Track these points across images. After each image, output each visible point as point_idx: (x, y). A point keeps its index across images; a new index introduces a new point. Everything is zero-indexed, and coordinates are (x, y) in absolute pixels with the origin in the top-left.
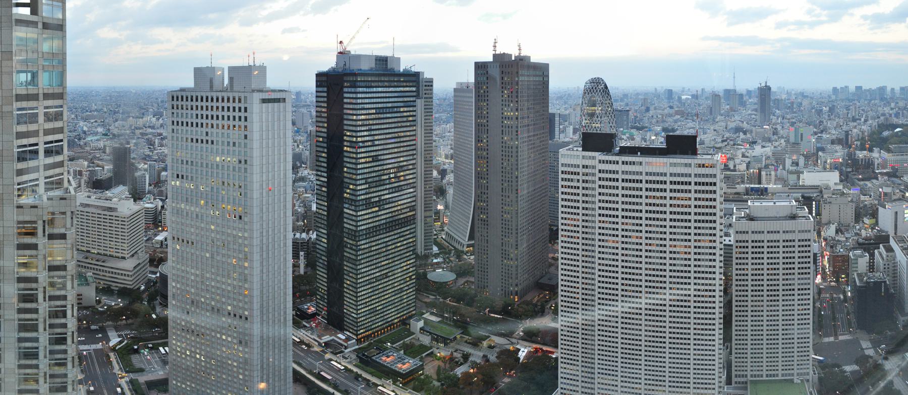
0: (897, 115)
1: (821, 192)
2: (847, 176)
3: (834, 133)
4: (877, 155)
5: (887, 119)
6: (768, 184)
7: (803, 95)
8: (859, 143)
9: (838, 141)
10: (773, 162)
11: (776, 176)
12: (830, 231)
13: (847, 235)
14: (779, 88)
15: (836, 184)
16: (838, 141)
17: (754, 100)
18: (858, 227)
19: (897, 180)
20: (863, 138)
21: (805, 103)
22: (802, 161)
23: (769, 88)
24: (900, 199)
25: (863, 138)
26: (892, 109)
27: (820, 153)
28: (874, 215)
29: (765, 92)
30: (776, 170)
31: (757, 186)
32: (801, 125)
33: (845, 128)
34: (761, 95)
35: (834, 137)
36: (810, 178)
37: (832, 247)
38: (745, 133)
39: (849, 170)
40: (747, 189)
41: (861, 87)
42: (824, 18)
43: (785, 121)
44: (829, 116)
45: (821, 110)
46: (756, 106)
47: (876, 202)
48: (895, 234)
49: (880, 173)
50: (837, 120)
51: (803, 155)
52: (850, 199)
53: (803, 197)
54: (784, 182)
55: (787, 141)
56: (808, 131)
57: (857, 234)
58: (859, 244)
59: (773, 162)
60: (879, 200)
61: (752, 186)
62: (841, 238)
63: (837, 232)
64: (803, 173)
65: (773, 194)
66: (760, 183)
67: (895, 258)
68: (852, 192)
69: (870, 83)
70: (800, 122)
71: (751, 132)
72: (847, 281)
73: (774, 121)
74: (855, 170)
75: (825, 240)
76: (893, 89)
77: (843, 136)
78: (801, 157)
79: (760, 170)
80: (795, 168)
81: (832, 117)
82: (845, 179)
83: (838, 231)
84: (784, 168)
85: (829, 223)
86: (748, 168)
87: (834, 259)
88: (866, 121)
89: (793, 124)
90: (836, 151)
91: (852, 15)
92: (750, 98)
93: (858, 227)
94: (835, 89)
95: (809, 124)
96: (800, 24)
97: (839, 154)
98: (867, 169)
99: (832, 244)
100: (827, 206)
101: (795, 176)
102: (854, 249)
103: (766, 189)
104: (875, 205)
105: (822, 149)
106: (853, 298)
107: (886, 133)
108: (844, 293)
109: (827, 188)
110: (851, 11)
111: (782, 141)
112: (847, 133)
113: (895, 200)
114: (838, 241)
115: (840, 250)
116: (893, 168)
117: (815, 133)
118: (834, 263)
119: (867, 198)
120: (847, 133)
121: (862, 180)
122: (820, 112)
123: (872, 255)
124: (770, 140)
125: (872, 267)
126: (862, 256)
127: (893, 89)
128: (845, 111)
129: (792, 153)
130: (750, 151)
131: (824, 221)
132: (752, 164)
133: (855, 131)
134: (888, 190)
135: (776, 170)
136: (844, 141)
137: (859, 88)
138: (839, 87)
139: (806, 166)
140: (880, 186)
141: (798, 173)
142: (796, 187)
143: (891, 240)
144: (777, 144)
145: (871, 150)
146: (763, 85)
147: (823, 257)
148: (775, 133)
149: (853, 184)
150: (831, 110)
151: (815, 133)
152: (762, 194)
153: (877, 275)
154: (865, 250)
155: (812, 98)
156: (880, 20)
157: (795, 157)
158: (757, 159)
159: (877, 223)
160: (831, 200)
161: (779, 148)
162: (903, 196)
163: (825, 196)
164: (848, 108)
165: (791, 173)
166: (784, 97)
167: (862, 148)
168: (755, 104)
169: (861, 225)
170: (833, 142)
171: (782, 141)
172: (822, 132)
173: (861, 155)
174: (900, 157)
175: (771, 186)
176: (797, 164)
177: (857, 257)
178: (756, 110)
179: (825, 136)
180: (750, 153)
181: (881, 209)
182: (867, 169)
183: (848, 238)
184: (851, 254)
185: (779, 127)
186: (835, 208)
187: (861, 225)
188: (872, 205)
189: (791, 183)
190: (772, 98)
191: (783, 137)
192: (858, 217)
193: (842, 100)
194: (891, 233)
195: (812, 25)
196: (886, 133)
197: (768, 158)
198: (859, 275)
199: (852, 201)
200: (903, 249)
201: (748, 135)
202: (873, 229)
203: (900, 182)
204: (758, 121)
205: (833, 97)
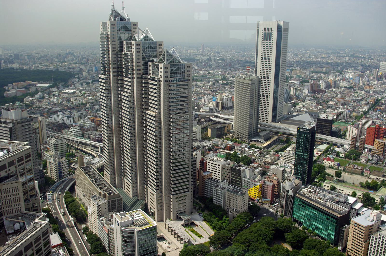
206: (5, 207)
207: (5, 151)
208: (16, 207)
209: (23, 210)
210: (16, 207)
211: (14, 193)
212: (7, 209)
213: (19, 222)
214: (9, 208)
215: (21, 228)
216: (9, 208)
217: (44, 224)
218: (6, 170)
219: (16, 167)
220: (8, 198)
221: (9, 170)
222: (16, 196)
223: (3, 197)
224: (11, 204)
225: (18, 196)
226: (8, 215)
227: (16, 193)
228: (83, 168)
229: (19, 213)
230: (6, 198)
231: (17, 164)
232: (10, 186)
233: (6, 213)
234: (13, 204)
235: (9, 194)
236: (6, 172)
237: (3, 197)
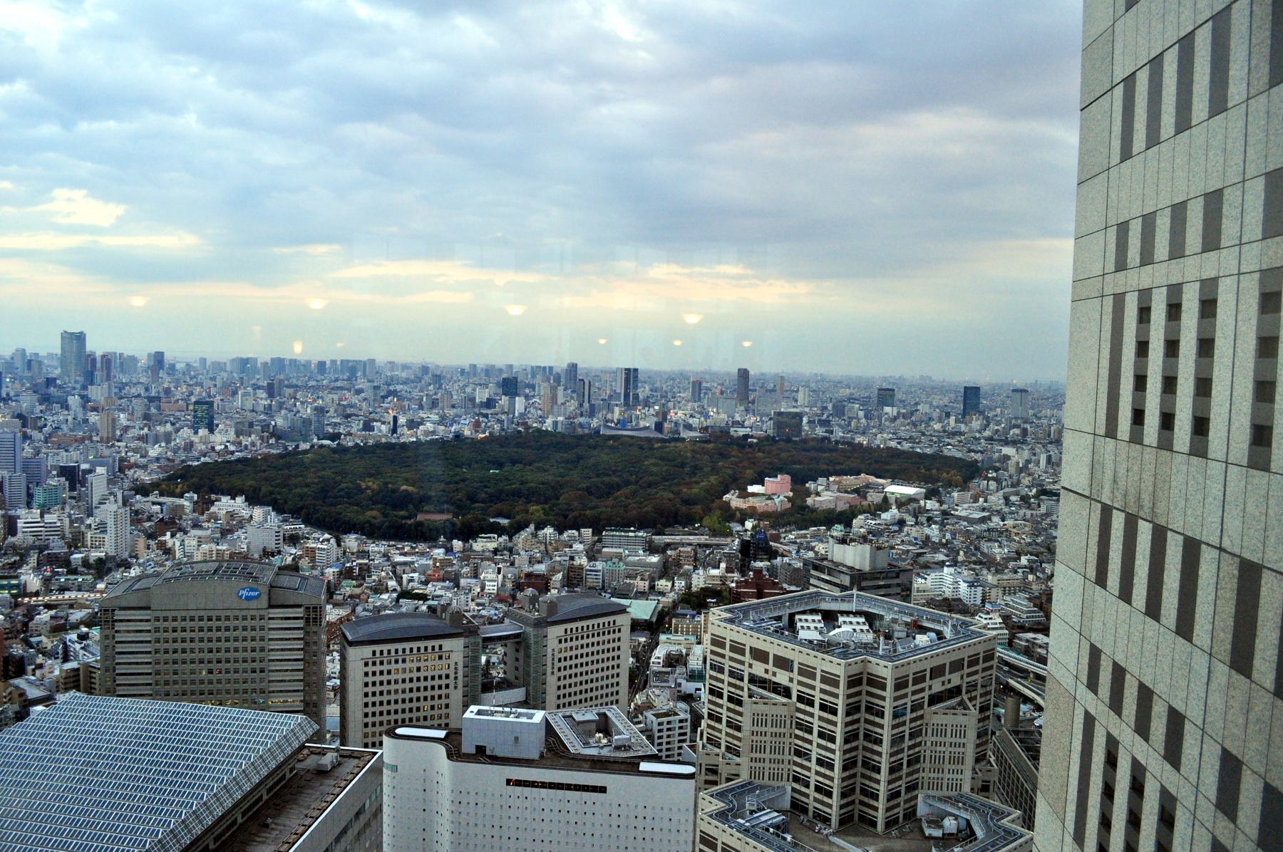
206: (927, 770)
207: (933, 635)
208: (951, 776)
209: (966, 789)
210: (951, 776)
211: (953, 740)
212: (932, 775)
213: (956, 817)
214: (936, 775)
215: (959, 831)
216: (936, 775)
217: (1021, 836)
218: (942, 679)
219: (962, 677)
220: (938, 749)
221: (949, 681)
222: (957, 750)
223: (929, 744)
224: (941, 766)
225: (961, 750)
226: (931, 792)
227: (958, 740)
228: (1016, 733)
229: (953, 793)
230: (933, 748)
231: (966, 671)
232: (949, 720)
233: (926, 786)
234: (947, 766)
235: (943, 739)
236: (943, 683)
237: (929, 744)
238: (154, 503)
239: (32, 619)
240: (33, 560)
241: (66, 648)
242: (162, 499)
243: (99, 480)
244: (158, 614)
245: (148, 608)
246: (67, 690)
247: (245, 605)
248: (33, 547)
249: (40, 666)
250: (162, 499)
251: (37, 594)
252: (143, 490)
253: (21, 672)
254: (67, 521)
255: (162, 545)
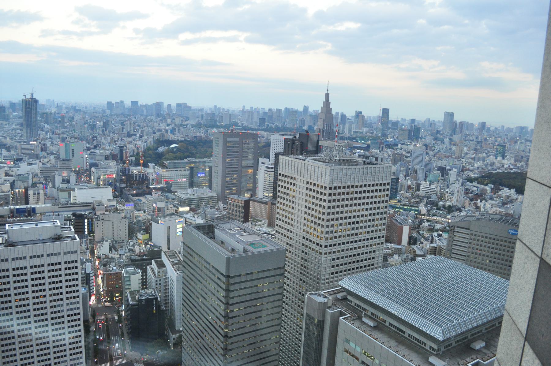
0: (173, 131)
1: (94, 209)
2: (121, 192)
3: (109, 149)
4: (152, 171)
5: (163, 135)
6: (37, 203)
7: (75, 109)
8: (134, 159)
9: (113, 157)
10: (42, 180)
11: (45, 194)
12: (103, 249)
13: (121, 252)
14: (48, 101)
15: (109, 200)
16: (113, 157)
17: (19, 113)
18: (131, 243)
19: (171, 196)
20: (138, 154)
21: (77, 117)
22: (73, 178)
23: (36, 101)
24: (173, 214)
25: (138, 154)
26: (168, 125)
27: (93, 169)
28: (148, 230)
29: (30, 105)
30: (45, 188)
31: (23, 207)
32: (72, 140)
33: (119, 144)
34: (26, 108)
35: (108, 153)
36: (82, 195)
37: (105, 265)
38: (8, 149)
39: (123, 185)
40: (11, 211)
41: (137, 102)
42: (93, 29)
43: (55, 136)
44: (103, 131)
45: (95, 126)
46: (21, 121)
47: (150, 217)
48: (169, 248)
49: (154, 188)
50: (111, 135)
51: (75, 172)
52: (123, 215)
53: (74, 215)
54: (54, 200)
55: (57, 157)
56: (79, 147)
57: (131, 250)
58: (133, 261)
59: (42, 180)
60: (152, 216)
61: (18, 207)
62: (115, 255)
63: (110, 250)
64: (74, 190)
65: (41, 214)
66: (27, 203)
67: (166, 273)
68: (125, 207)
69: (171, 100)
70: (72, 137)
71: (16, 148)
72: (121, 300)
73: (42, 136)
74: (129, 186)
75: (99, 258)
76: (169, 106)
77: (117, 152)
78: (73, 174)
79: (26, 190)
80: (66, 185)
81: (107, 132)
82: (119, 194)
83: (112, 248)
84: (54, 186)
85: (102, 240)
86: (12, 186)
87: (107, 278)
88: (141, 136)
89: (63, 140)
90: (110, 167)
91: (124, 27)
92: (14, 111)
93: (131, 243)
94: (109, 104)
95: (81, 139)
96: (67, 33)
97: (113, 169)
98: (141, 185)
99: (105, 263)
100: (100, 223)
101: (66, 194)
102: (127, 266)
103: (34, 209)
104: (149, 220)
105: (95, 165)
106: (126, 317)
107: (161, 149)
108: (119, 313)
109: (100, 204)
110: (122, 24)
111: (52, 157)
112: (122, 149)
113: (168, 215)
114: (112, 258)
115: (113, 268)
116: (167, 183)
117: (88, 149)
118: (107, 282)
119: (141, 213)
120: (122, 149)
121: (136, 195)
122: (93, 127)
123: (144, 272)
124: (37, 157)
125: (144, 283)
126: (134, 274)
127: (169, 106)
128: (120, 126)
129: (63, 170)
130: (15, 169)
131: (97, 239)
132: (17, 184)
133: (130, 146)
134: (162, 205)
135: (45, 188)
136: (118, 157)
137: (135, 103)
138: (113, 102)
139: (78, 182)
140: (153, 201)
141: (69, 190)
142: (67, 205)
143: (163, 255)
144: (45, 160)
145: (145, 165)
146: (28, 97)
147: (96, 277)
148: (44, 148)
149: (127, 200)
150: (106, 125)
151: (88, 149)
152: (29, 215)
153: (149, 291)
154: (138, 266)
155: (85, 113)
156: (150, 35)
157: (65, 174)
158: (23, 177)
159: (150, 239)
160: (104, 217)
161: (49, 165)
162: (176, 211)
163: (98, 213)
164: (123, 124)
165: (62, 190)
166: (53, 110)
167: (137, 164)
168: (20, 117)
169: (135, 241)
170: (107, 158)
171: (52, 157)
172: (95, 147)
173: (135, 170)
174: (174, 173)
175: (40, 206)
176: (68, 181)
177: (129, 274)
178: (21, 125)
179: (98, 151)
180: (15, 171)
181: (154, 224)
182: (141, 185)
183: (121, 255)
184: (123, 272)
185: (48, 143)
186: (108, 225)
187: (135, 241)
188: (146, 221)
189: (63, 201)
190: (40, 111)
191: (52, 153)
192: (132, 234)
193: (117, 115)
194: (164, 248)
195: (81, 35)
196: (161, 149)
197: (35, 176)
198: (132, 293)
199: (125, 217)
200: (173, 264)
201: (12, 152)
202: (146, 244)
203: (174, 197)
204: (24, 136)
205: (108, 112)
238: (474, 187)
239: (421, 224)
240: (424, 202)
241: (432, 238)
242: (478, 185)
243: (453, 174)
244: (473, 232)
245: (469, 229)
246: (431, 254)
247: (510, 236)
248: (425, 197)
249: (422, 243)
250: (478, 185)
251: (424, 215)
252: (471, 180)
253: (415, 243)
254: (439, 189)
255: (476, 205)
